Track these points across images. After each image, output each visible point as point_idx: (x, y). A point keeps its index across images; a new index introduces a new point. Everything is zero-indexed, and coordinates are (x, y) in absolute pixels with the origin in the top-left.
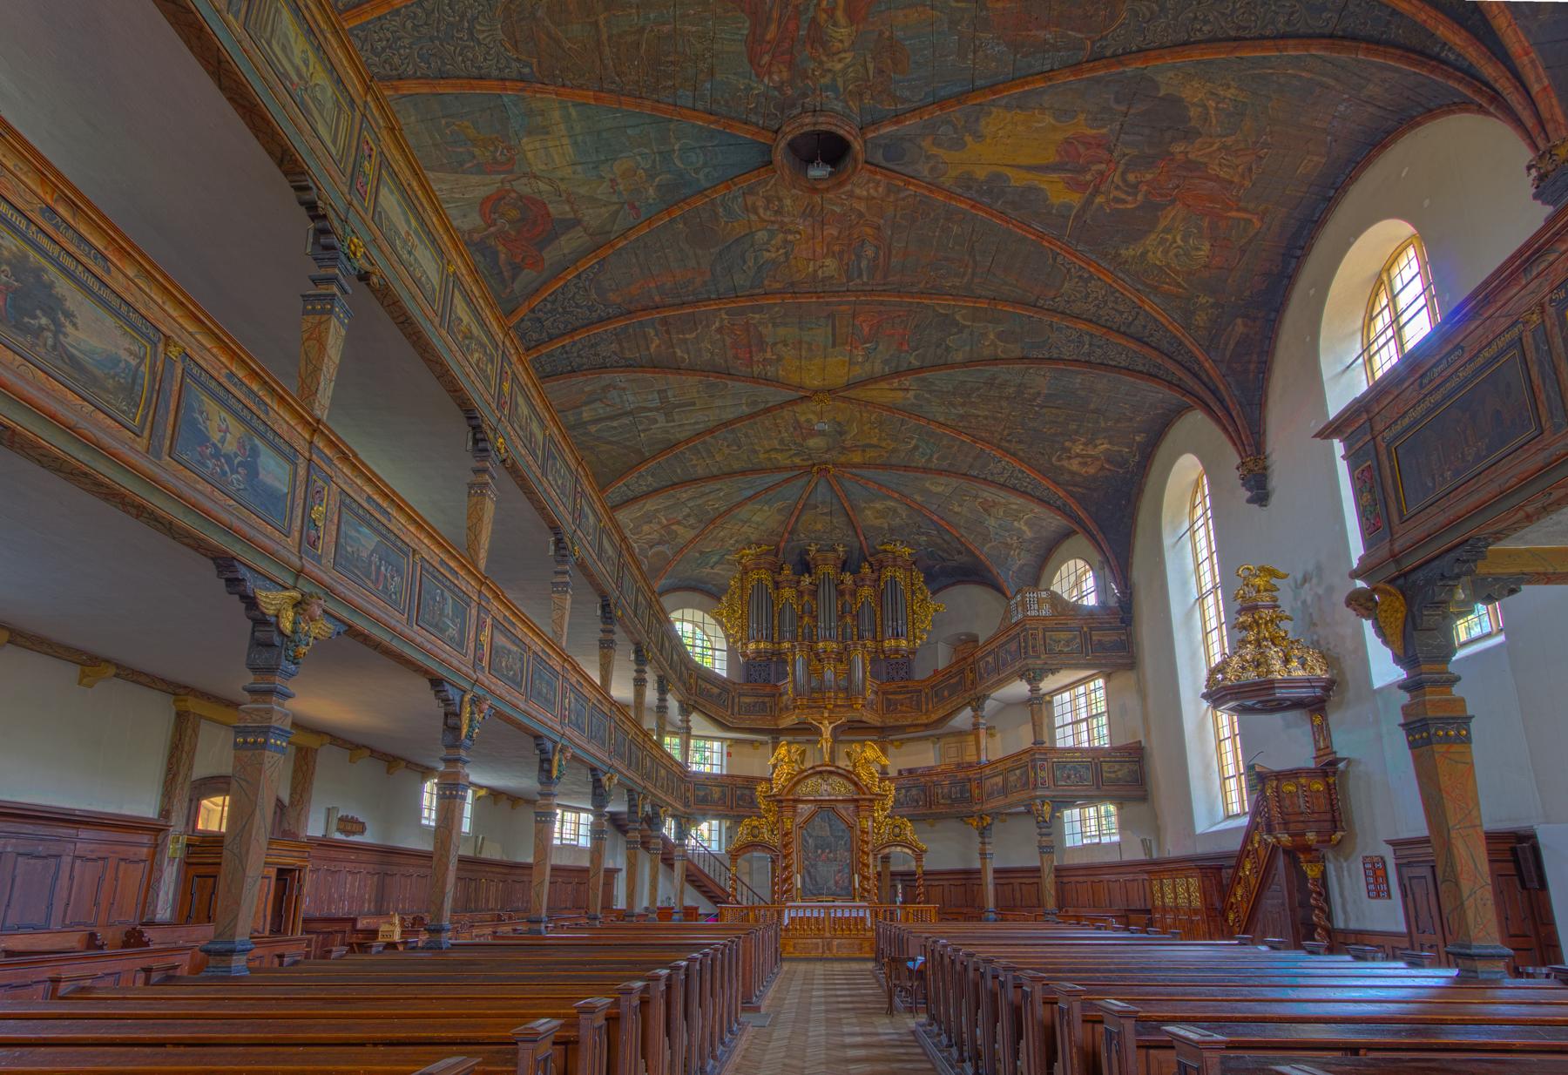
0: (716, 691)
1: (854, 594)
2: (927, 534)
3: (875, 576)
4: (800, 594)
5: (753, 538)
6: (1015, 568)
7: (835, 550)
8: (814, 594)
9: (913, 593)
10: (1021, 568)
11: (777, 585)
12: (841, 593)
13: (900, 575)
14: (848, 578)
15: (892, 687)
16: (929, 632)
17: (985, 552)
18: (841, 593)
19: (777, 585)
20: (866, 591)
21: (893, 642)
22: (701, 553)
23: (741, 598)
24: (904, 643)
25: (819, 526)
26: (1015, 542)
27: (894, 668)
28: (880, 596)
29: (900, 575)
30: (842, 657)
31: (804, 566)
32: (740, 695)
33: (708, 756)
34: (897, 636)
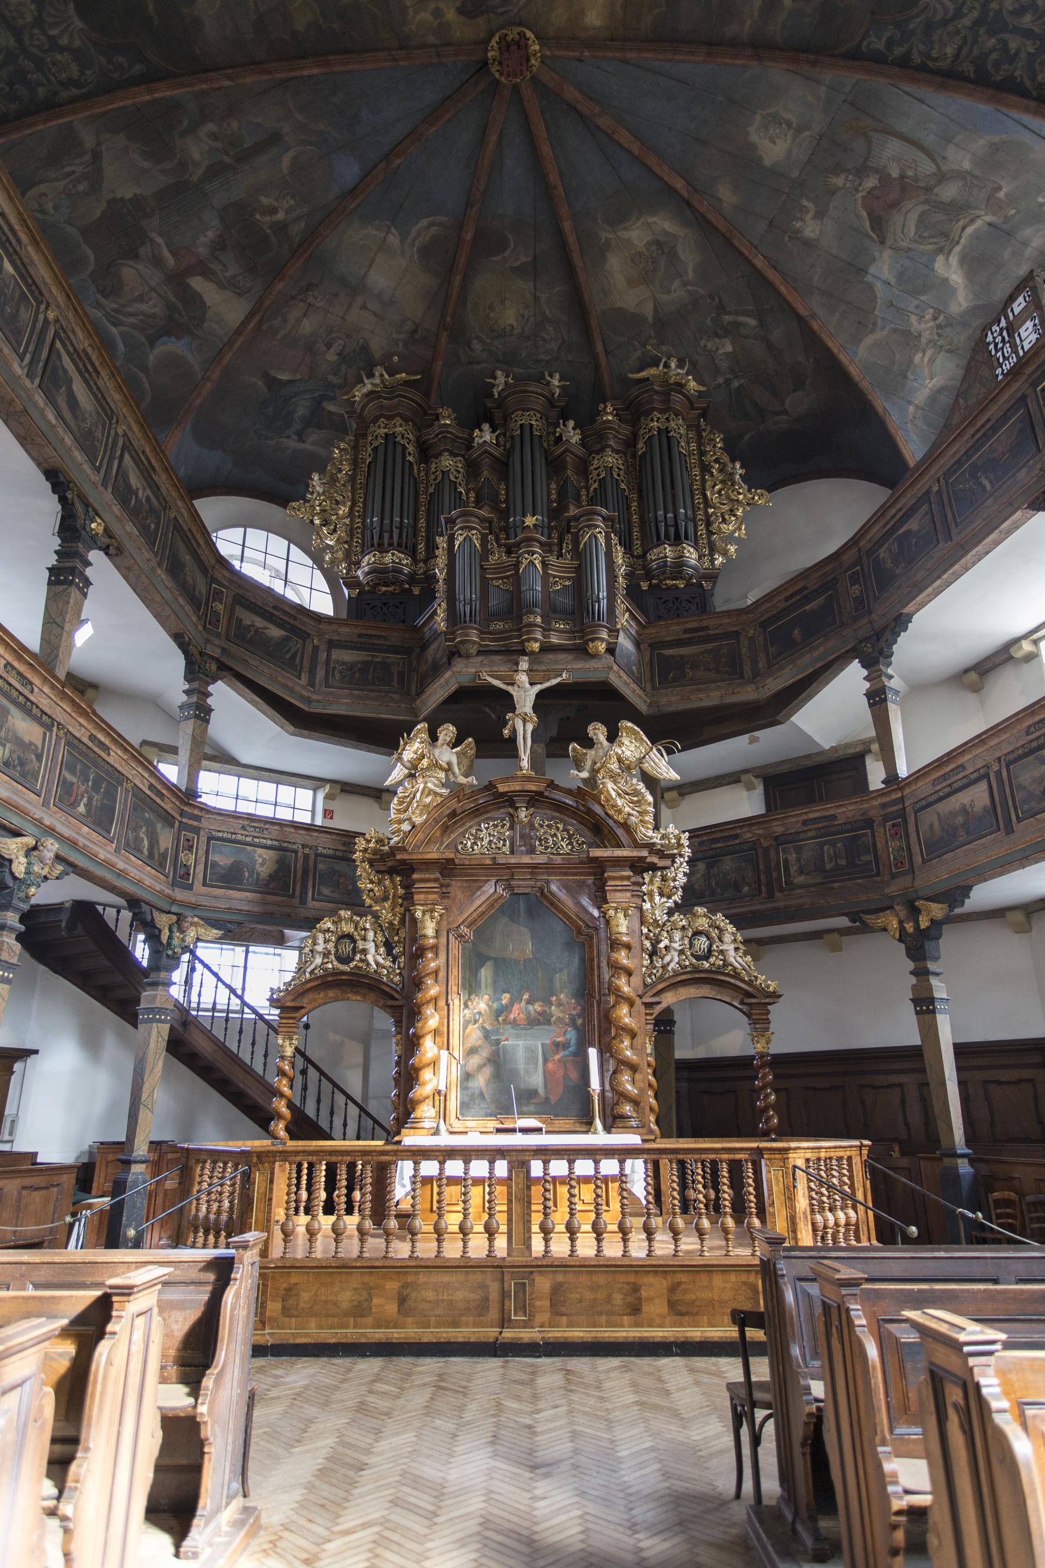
0: (276, 632)
1: (583, 468)
2: (731, 331)
3: (626, 430)
4: (472, 468)
5: (378, 345)
6: (921, 397)
7: (548, 383)
8: (503, 467)
9: (705, 469)
10: (932, 399)
11: (426, 453)
12: (555, 465)
13: (678, 427)
14: (572, 435)
15: (673, 629)
16: (738, 541)
17: (859, 357)
18: (555, 465)
19: (426, 453)
20: (611, 459)
21: (668, 551)
22: (272, 383)
23: (352, 479)
24: (691, 555)
25: (510, 316)
26: (923, 326)
27: (663, 598)
28: (639, 469)
29: (678, 427)
30: (563, 532)
31: (481, 409)
32: (332, 644)
33: (265, 779)
34: (677, 541)
